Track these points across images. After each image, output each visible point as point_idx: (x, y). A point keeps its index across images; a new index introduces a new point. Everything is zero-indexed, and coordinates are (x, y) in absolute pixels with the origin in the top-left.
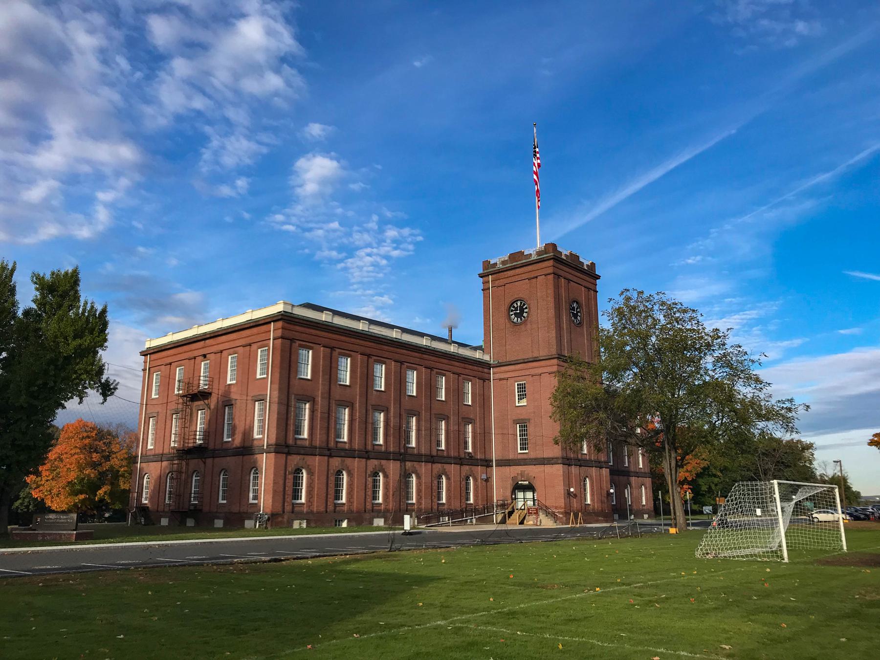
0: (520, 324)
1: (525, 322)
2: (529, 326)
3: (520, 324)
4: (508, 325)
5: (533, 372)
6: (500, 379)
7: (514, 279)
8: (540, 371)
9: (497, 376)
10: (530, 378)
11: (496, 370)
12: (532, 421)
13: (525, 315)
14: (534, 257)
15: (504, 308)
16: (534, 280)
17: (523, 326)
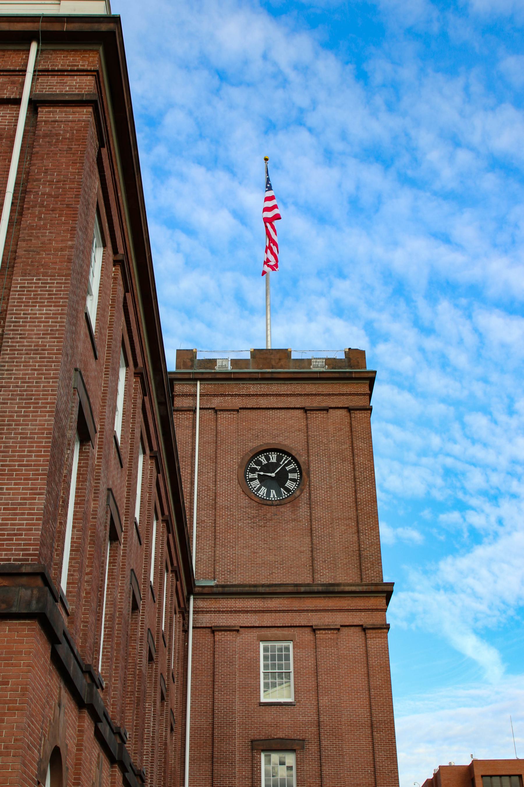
0: (280, 503)
1: (292, 500)
2: (303, 510)
3: (280, 503)
4: (244, 501)
5: (315, 620)
6: (213, 630)
7: (263, 402)
8: (339, 619)
9: (206, 620)
10: (307, 635)
11: (203, 604)
12: (313, 748)
13: (289, 484)
14: (318, 367)
15: (231, 461)
16: (320, 415)
17: (286, 510)
